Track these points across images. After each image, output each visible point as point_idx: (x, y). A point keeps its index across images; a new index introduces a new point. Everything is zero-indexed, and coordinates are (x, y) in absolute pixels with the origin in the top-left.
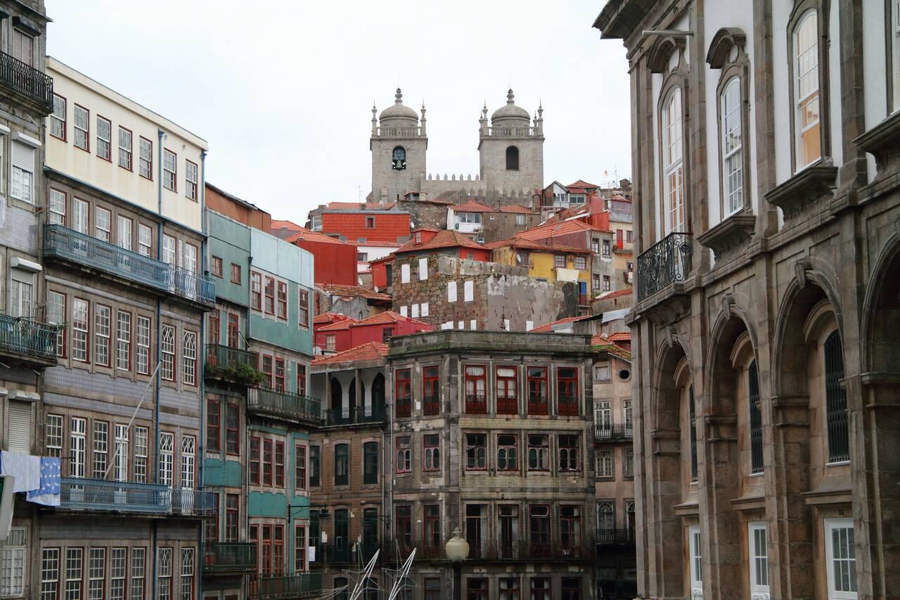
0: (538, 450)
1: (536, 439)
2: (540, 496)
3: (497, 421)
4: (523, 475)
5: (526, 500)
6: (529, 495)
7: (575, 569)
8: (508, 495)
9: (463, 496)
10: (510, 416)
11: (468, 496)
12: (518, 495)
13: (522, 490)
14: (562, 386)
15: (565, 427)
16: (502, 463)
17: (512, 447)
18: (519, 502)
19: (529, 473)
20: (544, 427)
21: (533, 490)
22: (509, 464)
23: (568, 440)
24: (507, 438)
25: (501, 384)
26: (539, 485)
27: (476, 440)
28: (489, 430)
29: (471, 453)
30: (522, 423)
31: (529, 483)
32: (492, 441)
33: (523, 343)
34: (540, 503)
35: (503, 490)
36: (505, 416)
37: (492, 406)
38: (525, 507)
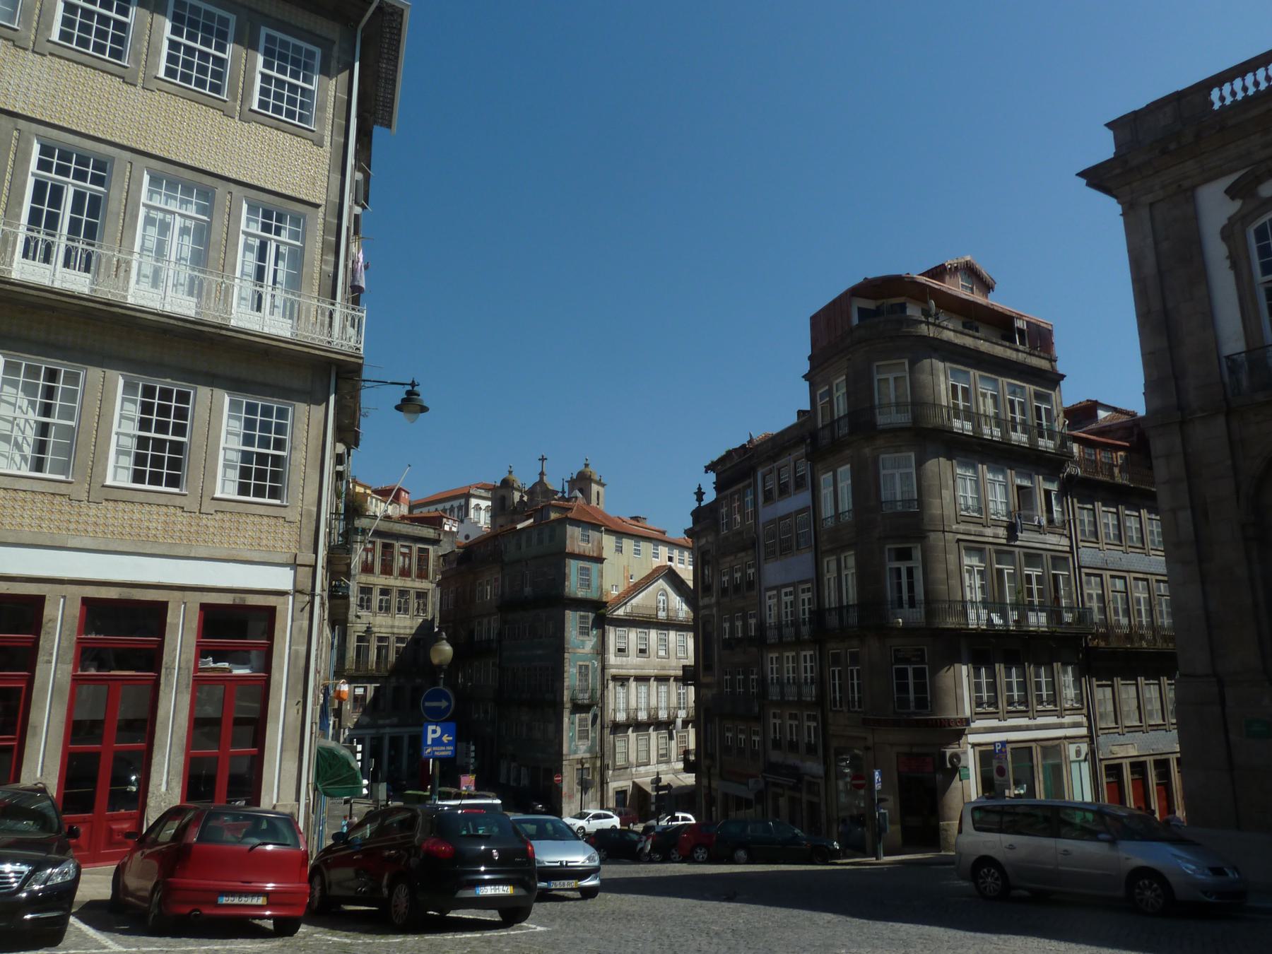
0: (403, 600)
1: (403, 593)
2: (402, 631)
3: (380, 579)
4: (393, 617)
5: (393, 634)
6: (396, 631)
7: (419, 681)
8: (383, 630)
9: (354, 629)
10: (388, 577)
11: (358, 629)
12: (389, 630)
13: (392, 627)
14: (420, 559)
15: (420, 587)
16: (381, 608)
17: (387, 597)
18: (389, 635)
19: (397, 616)
20: (407, 585)
21: (398, 627)
22: (385, 608)
23: (421, 595)
24: (385, 592)
25: (404, 557)
26: (402, 624)
27: (366, 590)
28: (374, 585)
29: (362, 599)
30: (394, 582)
31: (396, 623)
32: (376, 592)
33: (398, 528)
34: (402, 636)
35: (381, 626)
36: (385, 576)
37: (378, 567)
38: (393, 639)
